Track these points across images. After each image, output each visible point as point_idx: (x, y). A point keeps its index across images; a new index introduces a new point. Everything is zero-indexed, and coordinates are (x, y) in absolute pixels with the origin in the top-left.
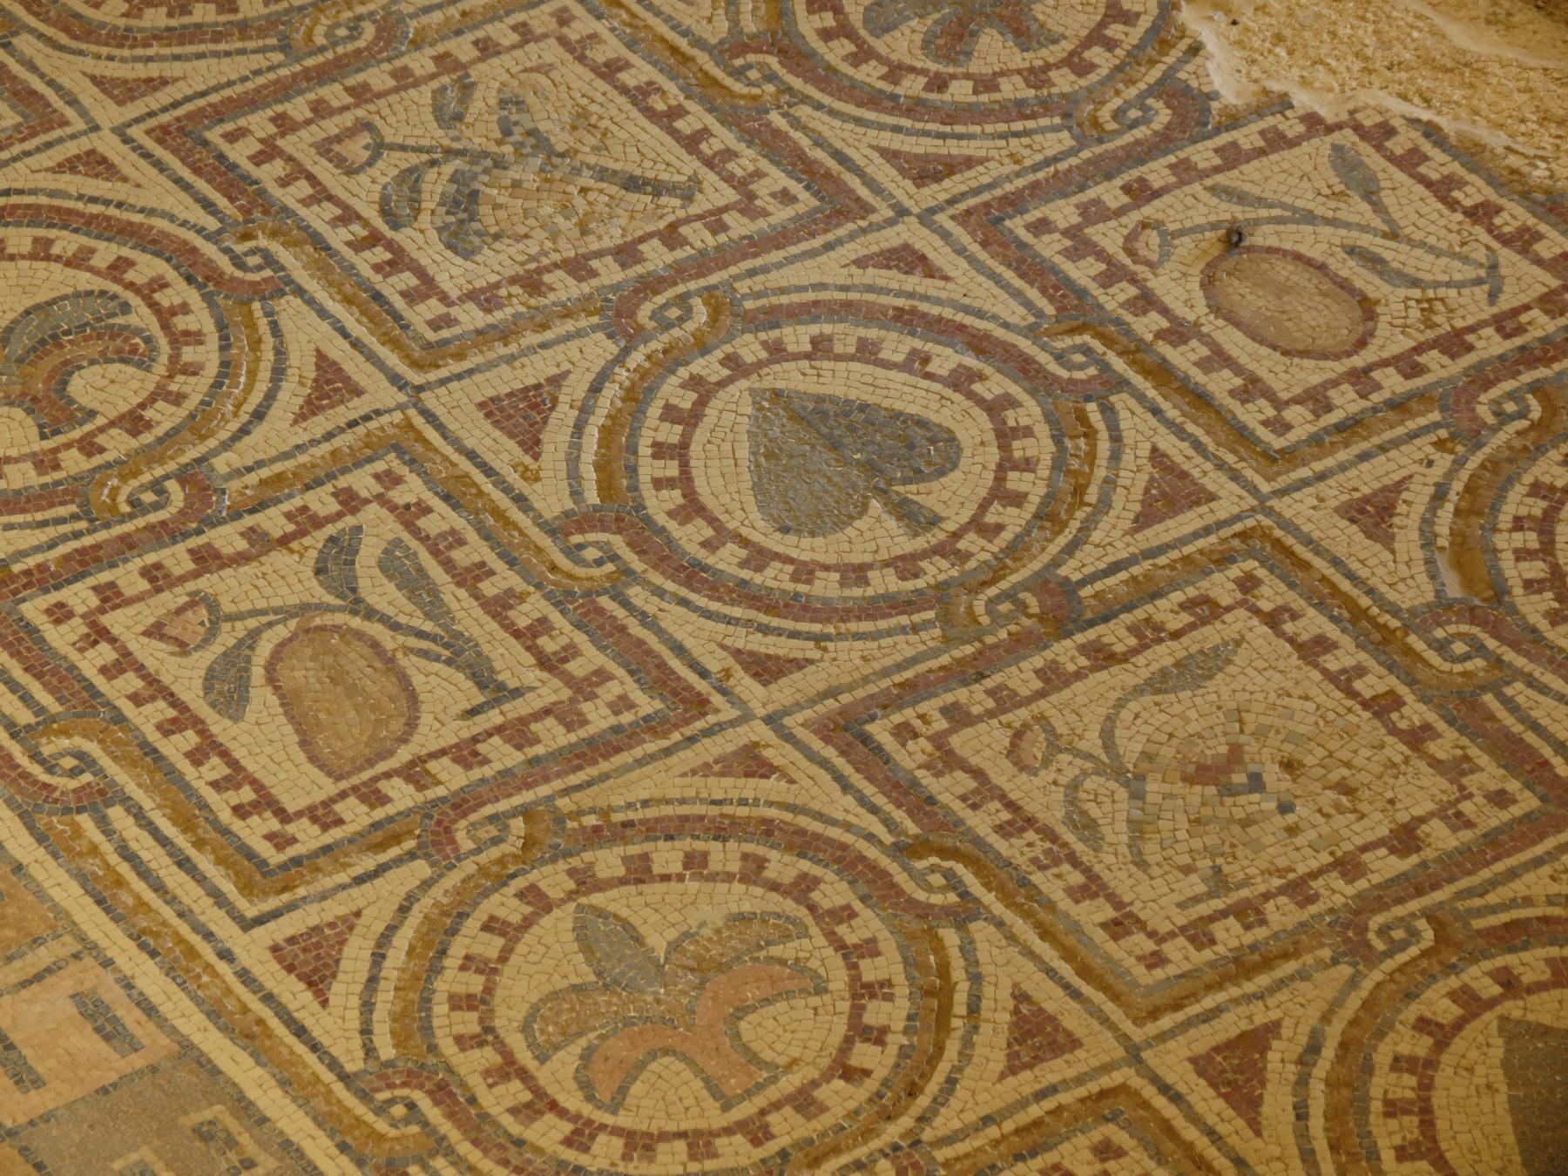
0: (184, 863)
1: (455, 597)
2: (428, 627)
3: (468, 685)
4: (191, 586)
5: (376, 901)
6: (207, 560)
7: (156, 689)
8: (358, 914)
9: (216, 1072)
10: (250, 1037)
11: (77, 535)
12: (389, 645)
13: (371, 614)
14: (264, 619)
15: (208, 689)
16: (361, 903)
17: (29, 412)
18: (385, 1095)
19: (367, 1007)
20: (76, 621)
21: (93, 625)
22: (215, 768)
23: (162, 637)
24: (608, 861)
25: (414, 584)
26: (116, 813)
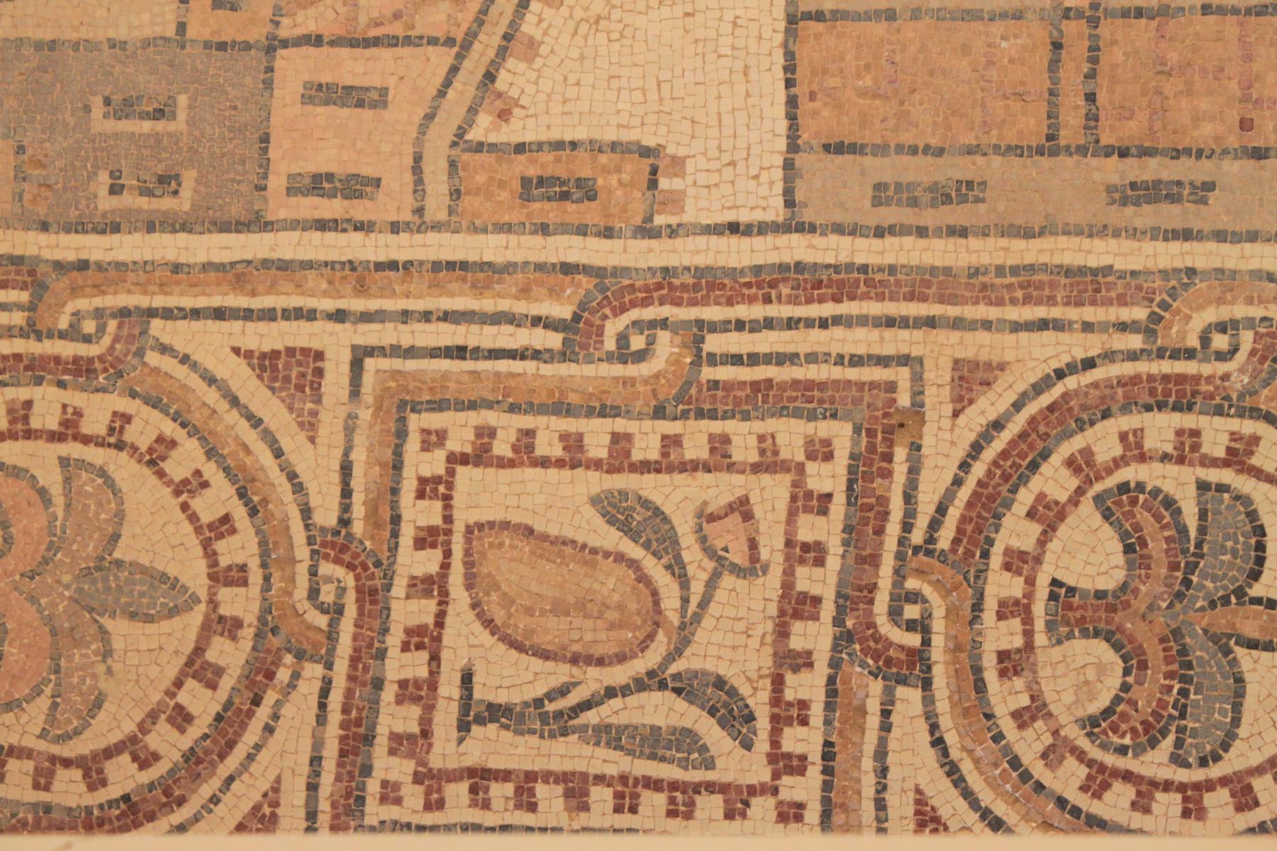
0: (460, 352)
1: (613, 762)
2: (591, 717)
3: (502, 698)
4: (776, 573)
5: (317, 462)
6: (798, 606)
7: (670, 461)
8: (312, 440)
9: (225, 227)
10: (236, 274)
11: (907, 527)
12: (593, 672)
14: (694, 601)
15: (645, 503)
16: (322, 450)
17: (1100, 595)
18: (112, 325)
19: (211, 380)
20: (800, 457)
21: (784, 467)
22: (547, 445)
23: (731, 508)
24: (232, 655)
25: (653, 742)
26: (554, 340)
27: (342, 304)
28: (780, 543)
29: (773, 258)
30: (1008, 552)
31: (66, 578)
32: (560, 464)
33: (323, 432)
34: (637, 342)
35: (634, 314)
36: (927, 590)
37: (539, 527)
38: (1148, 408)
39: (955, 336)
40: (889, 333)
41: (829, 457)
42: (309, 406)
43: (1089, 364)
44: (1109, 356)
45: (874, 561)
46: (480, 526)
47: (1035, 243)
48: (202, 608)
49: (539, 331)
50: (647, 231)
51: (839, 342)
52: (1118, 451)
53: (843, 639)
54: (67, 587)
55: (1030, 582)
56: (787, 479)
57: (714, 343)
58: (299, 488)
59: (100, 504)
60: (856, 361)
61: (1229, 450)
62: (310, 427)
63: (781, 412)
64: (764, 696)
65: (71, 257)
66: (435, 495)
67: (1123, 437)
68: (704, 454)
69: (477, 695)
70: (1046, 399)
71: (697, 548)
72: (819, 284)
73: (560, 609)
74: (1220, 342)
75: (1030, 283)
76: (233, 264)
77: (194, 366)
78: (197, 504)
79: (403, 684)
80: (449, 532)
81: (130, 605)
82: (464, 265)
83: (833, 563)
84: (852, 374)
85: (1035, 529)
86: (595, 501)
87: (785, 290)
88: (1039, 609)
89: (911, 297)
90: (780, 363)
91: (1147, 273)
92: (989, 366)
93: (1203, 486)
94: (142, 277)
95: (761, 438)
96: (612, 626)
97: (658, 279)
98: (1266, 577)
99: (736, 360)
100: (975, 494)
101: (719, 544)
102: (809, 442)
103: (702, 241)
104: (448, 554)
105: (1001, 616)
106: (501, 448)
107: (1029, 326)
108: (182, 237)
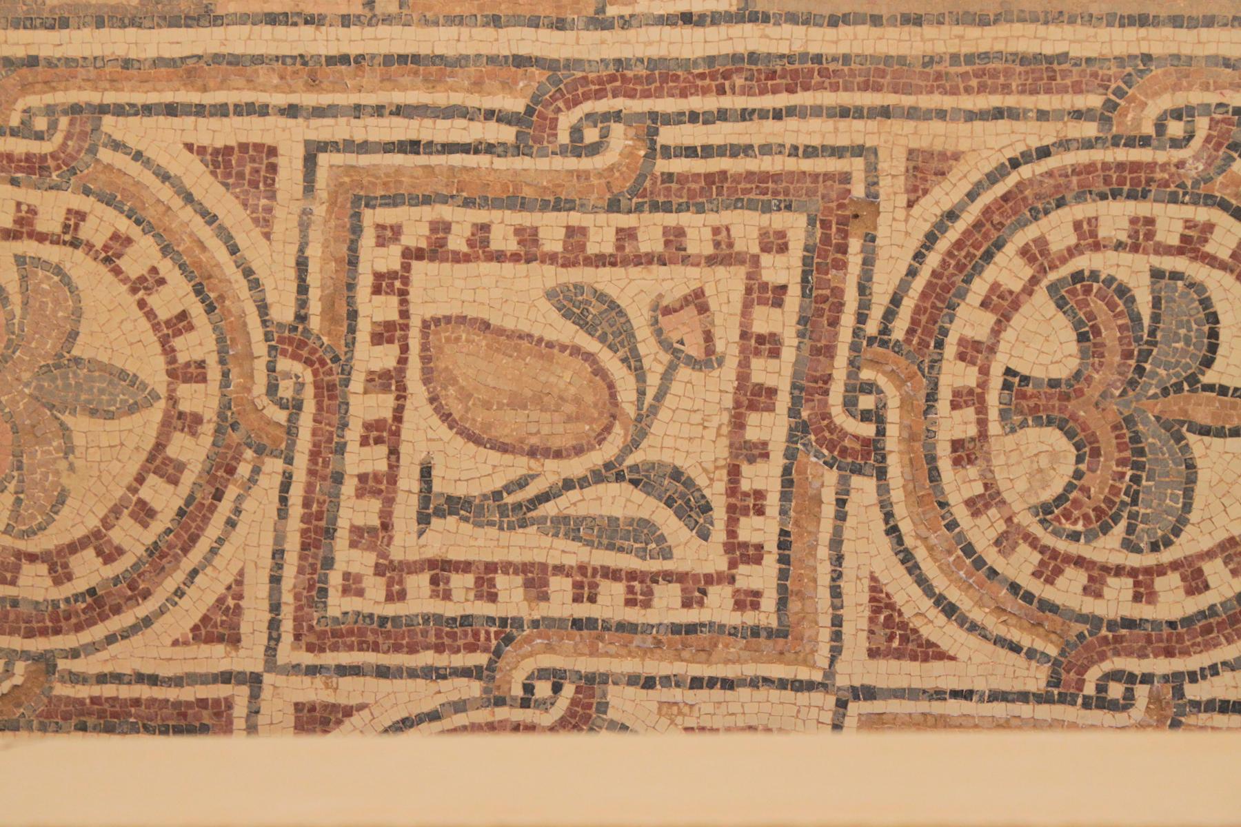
0: (413, 147)
1: (572, 553)
3: (460, 491)
4: (732, 363)
5: (272, 258)
6: (753, 397)
7: (624, 255)
8: (267, 236)
9: (174, 22)
10: (186, 69)
11: (862, 318)
12: (551, 464)
13: (598, 477)
14: (651, 393)
15: (601, 297)
16: (278, 246)
17: (1054, 383)
18: (64, 122)
19: (165, 177)
20: (755, 249)
21: (739, 259)
22: (502, 239)
23: (686, 301)
24: (191, 451)
25: (611, 533)
26: (507, 134)
27: (294, 99)
28: (735, 335)
29: (727, 49)
30: (962, 341)
31: (26, 376)
32: (515, 257)
33: (278, 228)
34: (591, 135)
35: (588, 107)
36: (882, 381)
37: (495, 321)
38: (1103, 197)
39: (910, 125)
40: (843, 124)
41: (783, 248)
42: (263, 202)
43: (1044, 152)
44: (1065, 144)
45: (829, 351)
46: (437, 321)
47: (990, 31)
48: (162, 404)
49: (492, 125)
50: (599, 22)
51: (794, 133)
52: (1072, 240)
53: (799, 430)
54: (27, 385)
55: (984, 371)
56: (742, 271)
57: (668, 136)
58: (255, 285)
59: (56, 302)
60: (811, 152)
61: (1185, 239)
62: (264, 223)
63: (737, 204)
64: (721, 486)
65: (20, 53)
66: (391, 290)
67: (1077, 226)
68: (659, 247)
69: (436, 488)
70: (1000, 189)
71: (652, 341)
72: (772, 75)
73: (517, 402)
74: (1176, 129)
75: (984, 71)
76: (183, 59)
77: (147, 163)
78: (154, 301)
79: (362, 478)
80: (405, 327)
81: (90, 402)
82: (416, 59)
83: (788, 354)
84: (807, 165)
85: (990, 319)
86: (550, 295)
87: (739, 81)
88: (993, 398)
89: (865, 87)
90: (734, 155)
91: (1103, 59)
92: (943, 156)
93: (1157, 274)
94: (93, 73)
95: (716, 231)
96: (569, 419)
97: (611, 70)
98: (1219, 363)
99: (690, 152)
100: (930, 285)
101: (674, 337)
102: (764, 234)
103: (655, 31)
104: (405, 349)
105: (955, 406)
106: (457, 242)
107: (983, 115)
108: (131, 31)
